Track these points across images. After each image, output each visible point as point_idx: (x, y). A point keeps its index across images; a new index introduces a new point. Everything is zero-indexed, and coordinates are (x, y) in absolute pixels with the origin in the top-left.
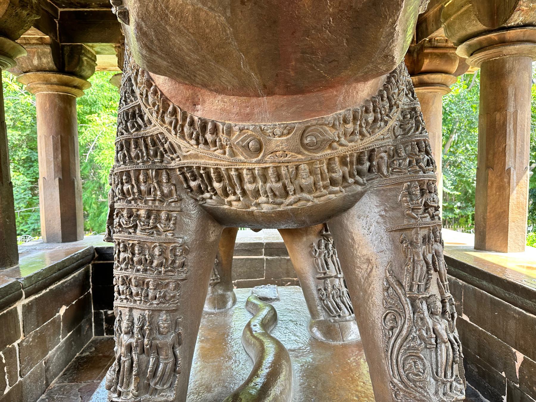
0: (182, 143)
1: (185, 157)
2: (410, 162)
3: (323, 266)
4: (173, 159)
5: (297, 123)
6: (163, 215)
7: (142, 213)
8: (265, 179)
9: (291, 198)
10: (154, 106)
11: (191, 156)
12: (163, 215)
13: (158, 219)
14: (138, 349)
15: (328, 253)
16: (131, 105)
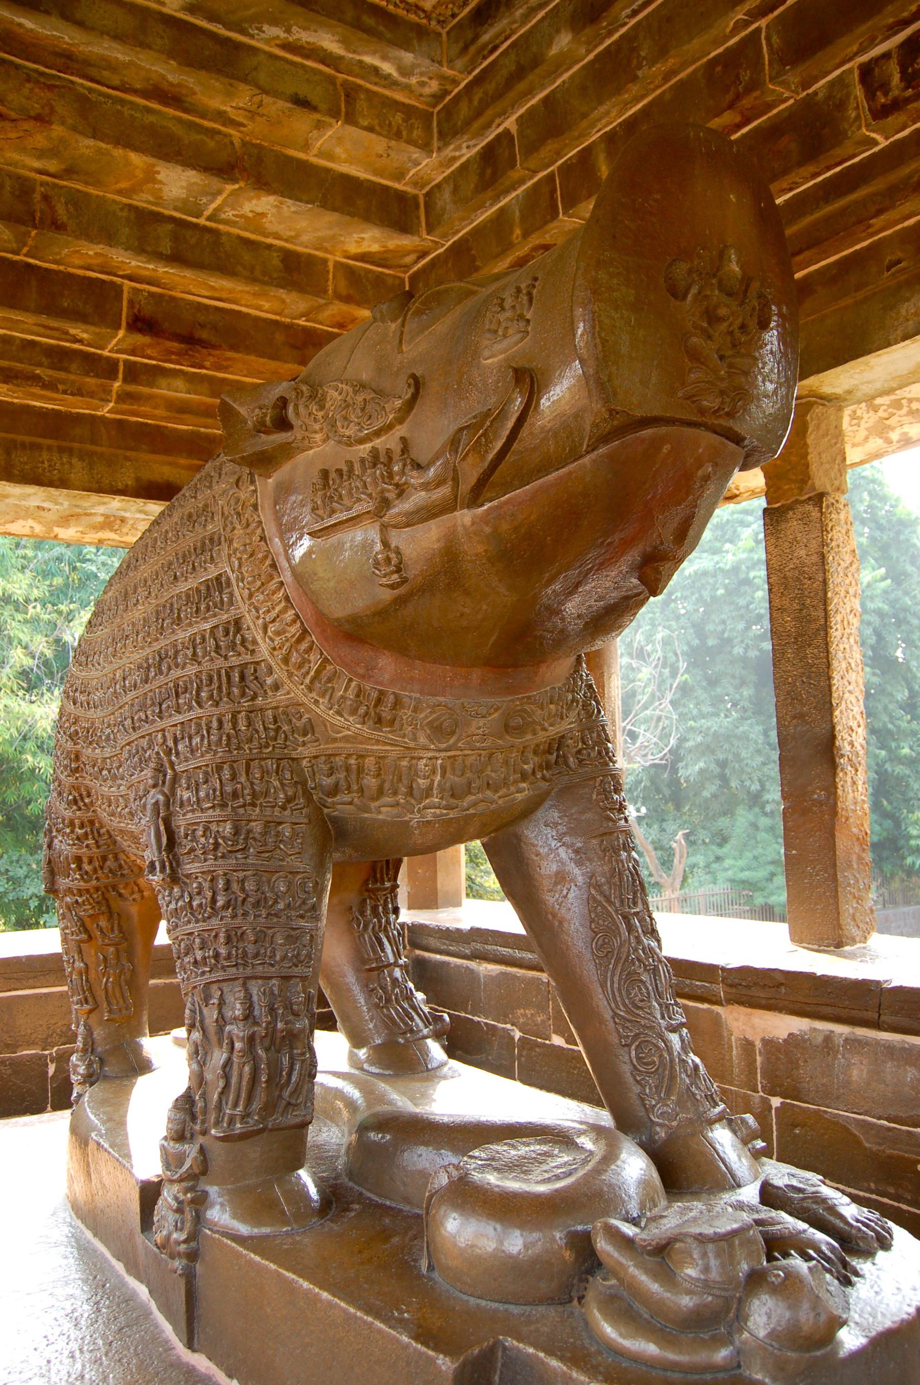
0: (338, 720)
1: (335, 740)
2: (599, 753)
3: (372, 947)
4: (304, 744)
10: (300, 666)
11: (346, 739)
14: (267, 1042)
15: (380, 922)
16: (234, 661)
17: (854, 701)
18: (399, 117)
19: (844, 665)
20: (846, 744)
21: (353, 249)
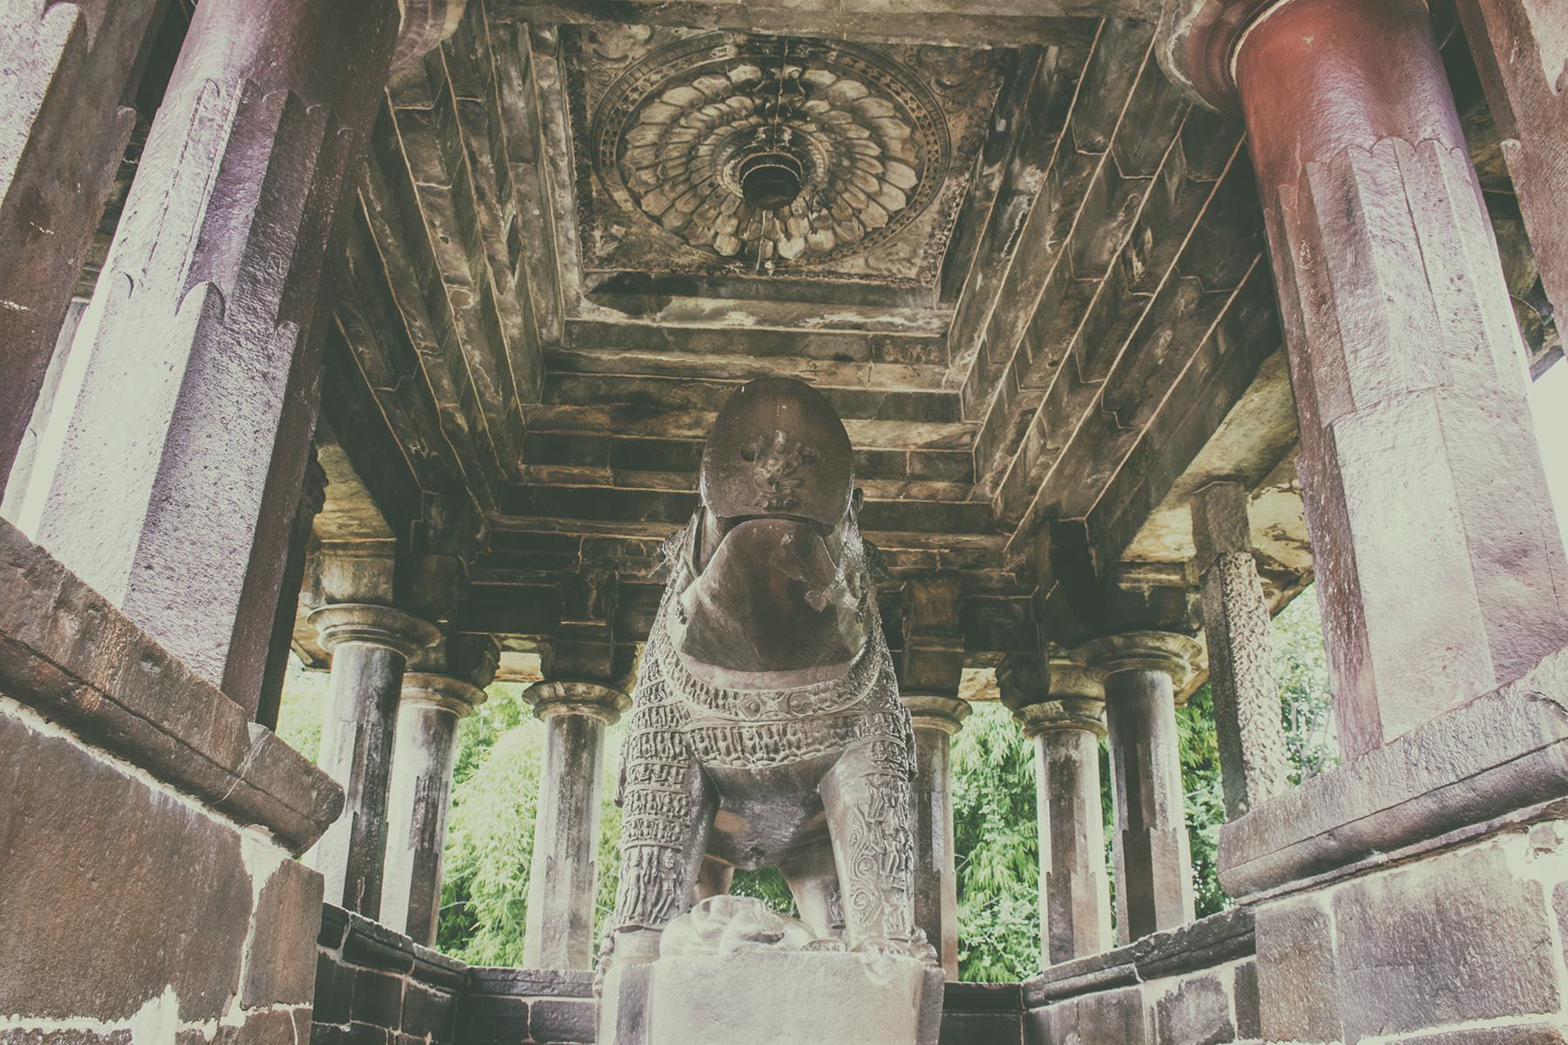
5: (787, 691)
6: (674, 771)
7: (657, 768)
8: (761, 738)
9: (782, 754)
12: (674, 771)
13: (669, 773)
17: (1267, 722)
18: (918, 348)
19: (1252, 693)
20: (1258, 758)
21: (920, 441)
